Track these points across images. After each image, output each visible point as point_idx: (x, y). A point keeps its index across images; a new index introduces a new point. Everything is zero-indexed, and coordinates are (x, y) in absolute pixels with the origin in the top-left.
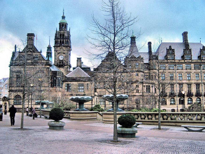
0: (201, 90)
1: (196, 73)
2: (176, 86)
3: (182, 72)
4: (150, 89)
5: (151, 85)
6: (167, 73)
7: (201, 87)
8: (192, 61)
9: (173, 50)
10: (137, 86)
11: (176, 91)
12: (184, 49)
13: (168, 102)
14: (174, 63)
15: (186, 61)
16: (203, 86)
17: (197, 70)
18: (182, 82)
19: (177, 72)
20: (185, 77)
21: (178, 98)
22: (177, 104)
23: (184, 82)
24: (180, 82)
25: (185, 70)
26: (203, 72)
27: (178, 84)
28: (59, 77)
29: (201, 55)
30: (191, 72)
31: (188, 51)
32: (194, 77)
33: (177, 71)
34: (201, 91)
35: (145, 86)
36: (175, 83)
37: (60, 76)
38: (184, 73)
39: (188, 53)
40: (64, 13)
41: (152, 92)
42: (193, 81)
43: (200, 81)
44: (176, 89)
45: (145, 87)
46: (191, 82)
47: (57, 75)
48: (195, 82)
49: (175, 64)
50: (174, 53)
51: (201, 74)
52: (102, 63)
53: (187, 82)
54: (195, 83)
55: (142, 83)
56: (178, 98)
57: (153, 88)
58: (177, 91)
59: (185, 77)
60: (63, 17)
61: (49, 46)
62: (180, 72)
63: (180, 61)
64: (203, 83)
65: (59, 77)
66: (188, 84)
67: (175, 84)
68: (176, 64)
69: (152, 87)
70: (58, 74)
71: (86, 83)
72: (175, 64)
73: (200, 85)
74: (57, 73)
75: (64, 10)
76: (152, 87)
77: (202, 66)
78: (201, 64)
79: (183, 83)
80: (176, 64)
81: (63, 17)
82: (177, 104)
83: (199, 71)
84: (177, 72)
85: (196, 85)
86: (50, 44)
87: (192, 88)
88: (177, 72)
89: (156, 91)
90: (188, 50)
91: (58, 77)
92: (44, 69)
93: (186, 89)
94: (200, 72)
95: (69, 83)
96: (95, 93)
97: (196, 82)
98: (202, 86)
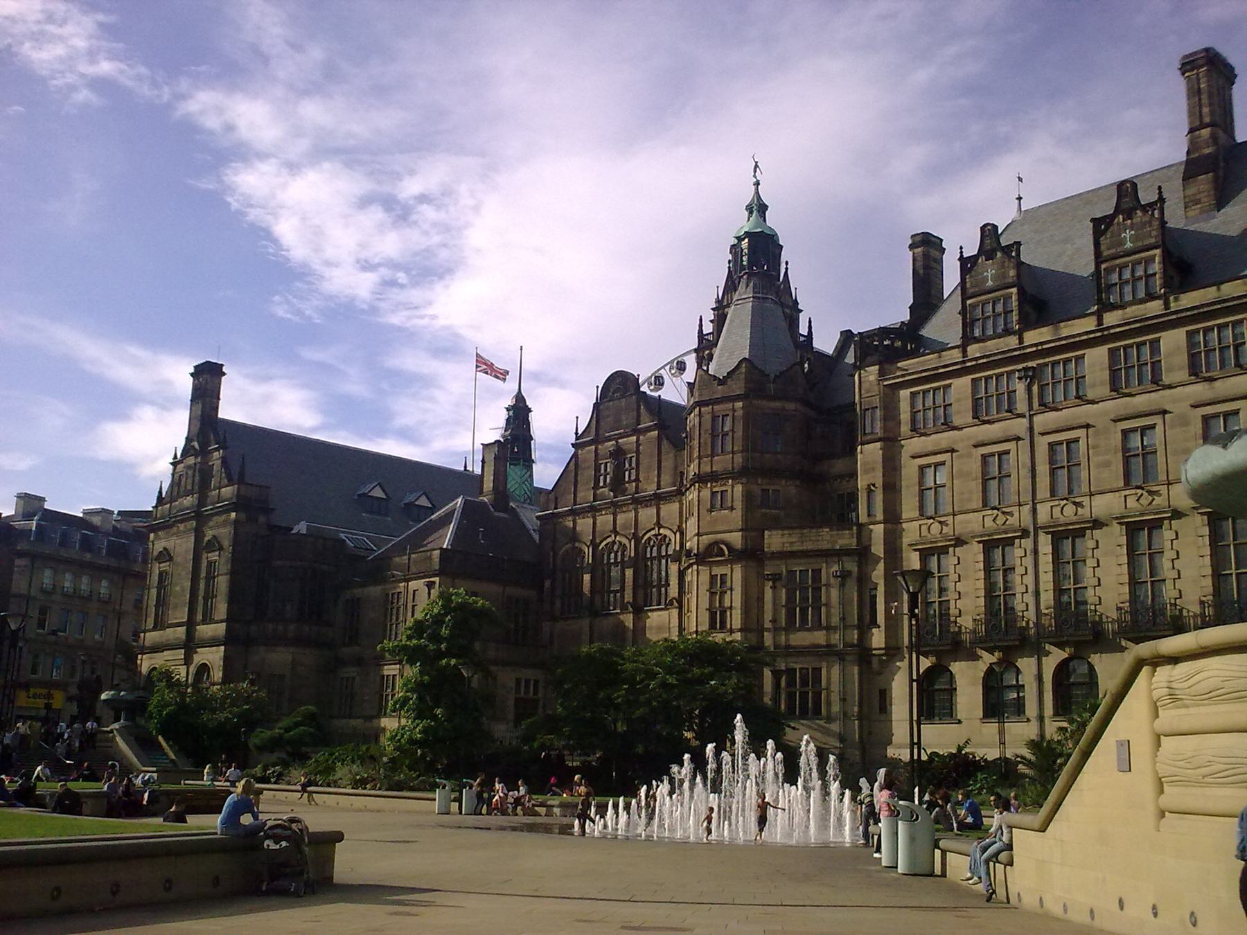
3: (1082, 421)
4: (817, 598)
9: (1007, 250)
12: (1093, 220)
15: (1111, 318)
20: (1107, 464)
22: (1041, 718)
30: (1164, 412)
35: (776, 578)
39: (1129, 245)
40: (757, 184)
41: (835, 620)
44: (1029, 580)
59: (1107, 464)
60: (759, 208)
62: (1064, 424)
72: (1026, 369)
75: (756, 166)
79: (1097, 524)
81: (759, 208)
82: (1041, 718)
91: (279, 563)
92: (223, 530)
95: (358, 592)
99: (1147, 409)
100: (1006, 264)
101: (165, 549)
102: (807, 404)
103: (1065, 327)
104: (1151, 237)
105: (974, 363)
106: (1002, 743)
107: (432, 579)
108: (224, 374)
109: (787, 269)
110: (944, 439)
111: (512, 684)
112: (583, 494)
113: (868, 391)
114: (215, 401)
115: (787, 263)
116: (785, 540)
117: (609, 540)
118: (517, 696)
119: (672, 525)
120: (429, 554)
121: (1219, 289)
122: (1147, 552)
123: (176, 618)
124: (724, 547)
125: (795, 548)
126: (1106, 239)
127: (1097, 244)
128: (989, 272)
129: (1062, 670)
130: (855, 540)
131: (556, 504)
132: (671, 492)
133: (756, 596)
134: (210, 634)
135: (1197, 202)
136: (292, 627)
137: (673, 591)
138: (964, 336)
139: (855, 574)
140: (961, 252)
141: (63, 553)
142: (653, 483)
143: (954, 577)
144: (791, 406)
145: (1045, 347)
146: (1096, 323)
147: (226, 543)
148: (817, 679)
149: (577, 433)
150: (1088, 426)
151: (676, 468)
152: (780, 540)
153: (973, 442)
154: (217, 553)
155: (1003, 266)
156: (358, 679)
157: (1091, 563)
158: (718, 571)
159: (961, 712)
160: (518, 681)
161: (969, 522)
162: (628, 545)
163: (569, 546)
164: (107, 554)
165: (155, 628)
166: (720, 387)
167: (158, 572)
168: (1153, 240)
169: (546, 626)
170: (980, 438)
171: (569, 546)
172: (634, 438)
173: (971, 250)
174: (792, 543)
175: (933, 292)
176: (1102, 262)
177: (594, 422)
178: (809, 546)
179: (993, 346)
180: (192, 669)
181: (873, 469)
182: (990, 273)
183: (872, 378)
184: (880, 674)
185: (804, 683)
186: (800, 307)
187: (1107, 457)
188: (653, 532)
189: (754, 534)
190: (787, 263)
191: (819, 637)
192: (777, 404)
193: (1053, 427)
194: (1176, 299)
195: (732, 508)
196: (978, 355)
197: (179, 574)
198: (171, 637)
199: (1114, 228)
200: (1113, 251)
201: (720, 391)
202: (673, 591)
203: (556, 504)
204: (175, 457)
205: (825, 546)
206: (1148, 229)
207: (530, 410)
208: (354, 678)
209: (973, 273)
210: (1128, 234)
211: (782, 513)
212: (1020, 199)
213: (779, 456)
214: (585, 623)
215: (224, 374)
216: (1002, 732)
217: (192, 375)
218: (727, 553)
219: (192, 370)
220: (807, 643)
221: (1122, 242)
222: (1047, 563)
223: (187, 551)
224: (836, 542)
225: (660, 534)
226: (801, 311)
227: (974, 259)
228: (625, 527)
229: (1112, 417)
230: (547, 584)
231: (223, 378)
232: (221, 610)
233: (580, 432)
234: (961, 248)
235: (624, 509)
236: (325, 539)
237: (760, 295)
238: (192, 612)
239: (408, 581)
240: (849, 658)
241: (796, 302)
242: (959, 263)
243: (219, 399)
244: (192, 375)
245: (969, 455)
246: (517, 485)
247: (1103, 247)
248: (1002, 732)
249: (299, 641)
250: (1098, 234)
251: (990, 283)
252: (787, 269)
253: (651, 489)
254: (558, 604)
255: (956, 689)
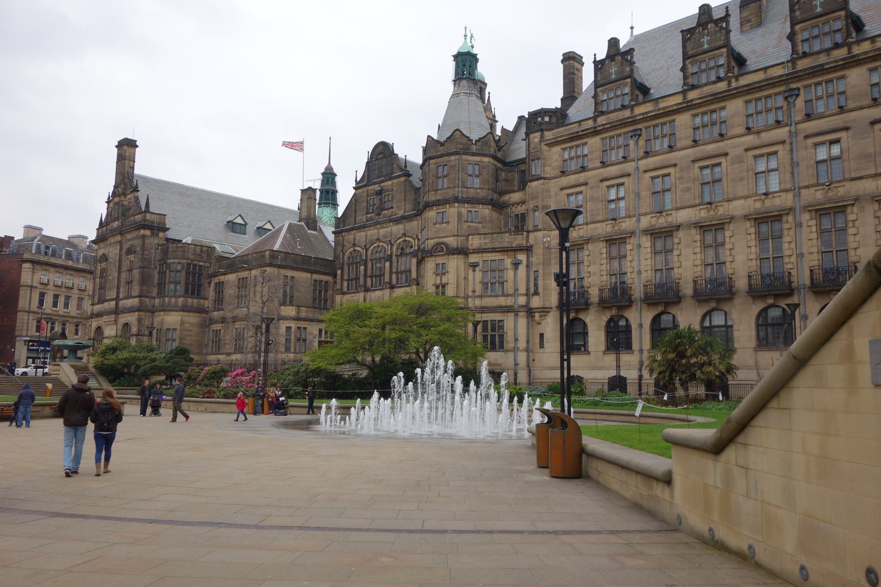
0: (787, 253)
1: (757, 152)
2: (639, 246)
3: (673, 162)
5: (508, 262)
6: (592, 188)
7: (792, 232)
8: (729, 84)
10: (441, 271)
11: (634, 275)
12: (682, 31)
13: (596, 337)
14: (623, 124)
15: (692, 95)
16: (805, 229)
17: (763, 135)
18: (670, 219)
19: (642, 169)
21: (644, 314)
23: (682, 216)
24: (662, 221)
25: (690, 151)
26: (806, 137)
27: (649, 237)
28: (177, 261)
29: (797, 27)
30: (726, 154)
31: (708, 35)
32: (741, 179)
33: (644, 163)
34: (793, 259)
35: (474, 266)
36: (633, 233)
37: (179, 259)
38: (682, 170)
39: (706, 46)
41: (511, 291)
42: (735, 203)
43: (787, 200)
44: (635, 264)
45: (477, 269)
46: (721, 211)
47: (170, 256)
48: (746, 212)
49: (632, 128)
50: (628, 69)
51: (792, 151)
52: (358, 191)
53: (702, 214)
54: (746, 217)
55: (463, 251)
56: (648, 316)
57: (522, 269)
58: (644, 274)
61: (326, 169)
62: (658, 165)
63: (662, 105)
64: (806, 208)
65: (177, 261)
66: (703, 228)
67: (632, 240)
68: (638, 126)
69: (516, 265)
70: (173, 251)
71: (254, 272)
72: (635, 130)
73: (786, 226)
74: (170, 250)
76: (516, 265)
77: (800, 103)
78: (794, 86)
79: (678, 227)
80: (638, 126)
83: (782, 133)
84: (645, 172)
85: (753, 230)
86: (332, 164)
87: (728, 246)
88: (645, 172)
89: (536, 285)
90: (709, 26)
91: (172, 261)
93: (693, 257)
94: (784, 142)
95: (222, 278)
96: (282, 307)
97: (758, 205)
98: (799, 225)
99: (716, 153)
100: (624, 64)
101: (104, 254)
102: (495, 158)
103: (662, 102)
104: (720, 40)
105: (602, 128)
106: (618, 367)
107: (265, 269)
108: (137, 146)
109: (489, 97)
110: (581, 177)
111: (317, 333)
112: (360, 218)
113: (534, 148)
114: (131, 163)
115: (489, 93)
116: (482, 242)
117: (375, 245)
118: (320, 339)
119: (413, 234)
120: (263, 253)
121: (765, 72)
122: (714, 245)
123: (110, 296)
124: (443, 247)
125: (488, 246)
126: (691, 43)
127: (684, 47)
128: (613, 70)
129: (656, 320)
130: (525, 241)
131: (344, 224)
132: (410, 215)
133: (463, 276)
134: (130, 305)
135: (749, 21)
136: (181, 300)
137: (414, 275)
138: (596, 110)
139: (525, 262)
140: (595, 58)
141: (53, 260)
142: (402, 209)
143: (586, 263)
144: (486, 159)
145: (649, 115)
146: (682, 99)
147: (138, 249)
148: (502, 327)
149: (356, 181)
150: (675, 165)
151: (415, 200)
152: (478, 242)
153: (600, 178)
154: (133, 256)
155: (622, 66)
156: (222, 331)
157: (676, 252)
158: (440, 260)
159: (591, 346)
160: (320, 331)
161: (597, 228)
162: (387, 248)
163: (352, 249)
164: (83, 262)
165: (99, 303)
166: (442, 148)
167: (99, 268)
168: (722, 42)
169: (338, 298)
170: (605, 176)
171: (352, 249)
172: (390, 183)
173: (602, 55)
174: (486, 243)
175: (576, 90)
176: (688, 58)
177: (366, 172)
178: (497, 245)
179: (613, 116)
180: (120, 327)
181: (537, 197)
182: (613, 70)
183: (537, 140)
184: (539, 324)
185: (493, 330)
186: (497, 119)
187: (689, 185)
188: (401, 239)
189: (462, 238)
190: (489, 93)
191: (502, 301)
192: (477, 158)
193: (652, 167)
194: (737, 80)
195: (448, 222)
196: (604, 122)
197: (111, 269)
198: (107, 307)
199: (696, 36)
200: (695, 51)
201: (442, 150)
202: (414, 275)
203: (344, 224)
204: (109, 197)
205: (506, 245)
206: (719, 35)
207: (335, 175)
208: (220, 330)
209: (603, 71)
210: (706, 39)
211: (480, 226)
212: (632, 28)
213: (478, 191)
214: (362, 295)
215: (137, 146)
216: (618, 360)
217: (116, 147)
218: (445, 250)
219: (117, 144)
220: (495, 305)
221: (701, 45)
222: (647, 253)
223: (115, 255)
224: (513, 242)
225: (406, 241)
226: (497, 122)
227: (602, 62)
228: (385, 236)
229: (692, 158)
230: (339, 272)
231: (137, 149)
232: (136, 290)
233: (358, 180)
234: (595, 55)
235: (385, 226)
236: (202, 246)
237: (468, 92)
238: (118, 293)
239: (250, 270)
240: (520, 314)
241: (494, 116)
242: (593, 65)
243: (134, 162)
244: (116, 147)
245: (598, 187)
246: (328, 219)
247: (688, 49)
248: (618, 360)
249: (185, 309)
250: (685, 42)
251: (613, 76)
252: (489, 97)
253: (401, 213)
254: (345, 284)
255: (587, 333)
